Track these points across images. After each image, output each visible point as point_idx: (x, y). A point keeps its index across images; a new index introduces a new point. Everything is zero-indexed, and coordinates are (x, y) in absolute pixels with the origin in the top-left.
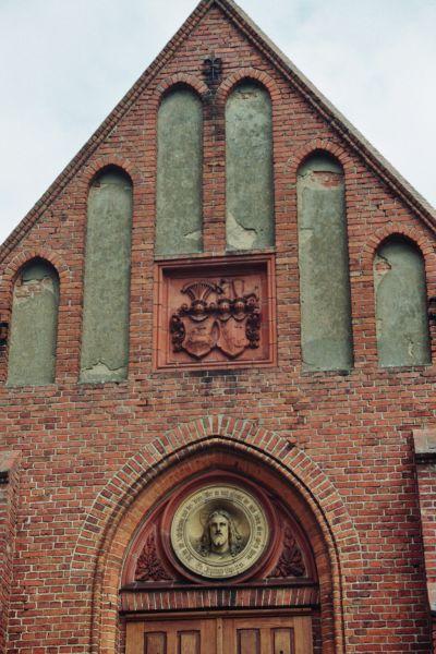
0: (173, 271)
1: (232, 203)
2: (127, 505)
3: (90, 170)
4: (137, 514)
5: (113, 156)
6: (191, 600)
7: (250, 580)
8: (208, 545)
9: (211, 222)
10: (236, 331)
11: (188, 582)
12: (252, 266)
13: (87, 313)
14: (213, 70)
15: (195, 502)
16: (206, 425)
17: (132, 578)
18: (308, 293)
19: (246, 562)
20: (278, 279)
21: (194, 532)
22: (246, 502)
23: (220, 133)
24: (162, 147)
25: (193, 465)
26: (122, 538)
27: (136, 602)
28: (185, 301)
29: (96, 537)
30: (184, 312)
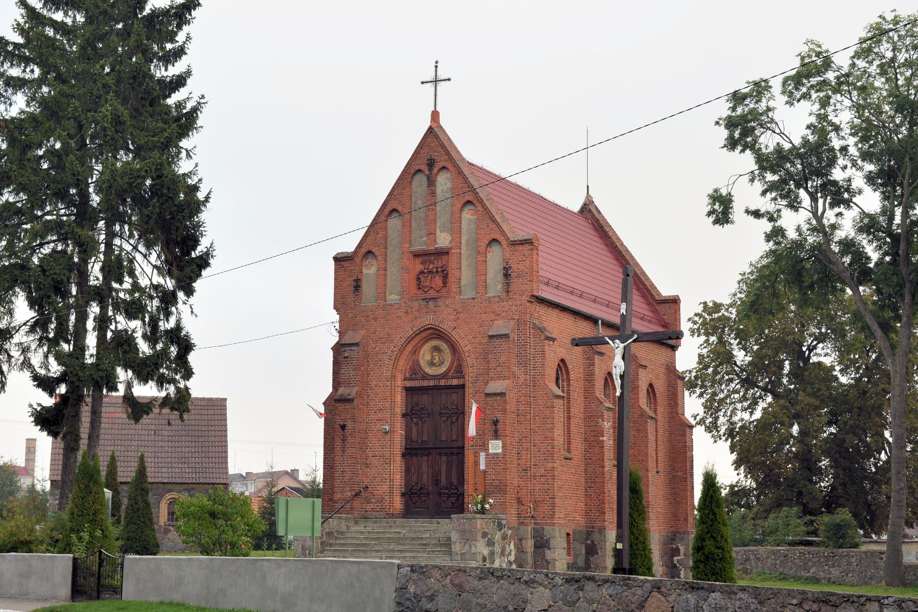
0: (416, 255)
1: (438, 224)
2: (401, 351)
3: (386, 211)
4: (406, 353)
5: (394, 204)
6: (425, 383)
7: (444, 376)
8: (431, 364)
9: (432, 234)
10: (438, 280)
11: (426, 377)
12: (443, 253)
13: (388, 273)
14: (431, 163)
15: (427, 347)
16: (427, 320)
17: (408, 375)
18: (464, 263)
19: (443, 369)
20: (453, 258)
21: (428, 357)
22: (444, 346)
23: (433, 193)
24: (413, 199)
25: (424, 335)
26: (402, 362)
27: (409, 384)
28: (421, 267)
29: (392, 362)
30: (422, 272)
